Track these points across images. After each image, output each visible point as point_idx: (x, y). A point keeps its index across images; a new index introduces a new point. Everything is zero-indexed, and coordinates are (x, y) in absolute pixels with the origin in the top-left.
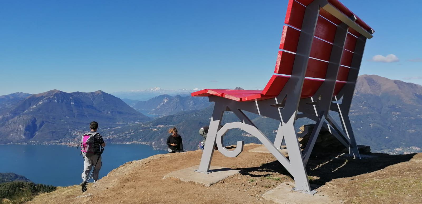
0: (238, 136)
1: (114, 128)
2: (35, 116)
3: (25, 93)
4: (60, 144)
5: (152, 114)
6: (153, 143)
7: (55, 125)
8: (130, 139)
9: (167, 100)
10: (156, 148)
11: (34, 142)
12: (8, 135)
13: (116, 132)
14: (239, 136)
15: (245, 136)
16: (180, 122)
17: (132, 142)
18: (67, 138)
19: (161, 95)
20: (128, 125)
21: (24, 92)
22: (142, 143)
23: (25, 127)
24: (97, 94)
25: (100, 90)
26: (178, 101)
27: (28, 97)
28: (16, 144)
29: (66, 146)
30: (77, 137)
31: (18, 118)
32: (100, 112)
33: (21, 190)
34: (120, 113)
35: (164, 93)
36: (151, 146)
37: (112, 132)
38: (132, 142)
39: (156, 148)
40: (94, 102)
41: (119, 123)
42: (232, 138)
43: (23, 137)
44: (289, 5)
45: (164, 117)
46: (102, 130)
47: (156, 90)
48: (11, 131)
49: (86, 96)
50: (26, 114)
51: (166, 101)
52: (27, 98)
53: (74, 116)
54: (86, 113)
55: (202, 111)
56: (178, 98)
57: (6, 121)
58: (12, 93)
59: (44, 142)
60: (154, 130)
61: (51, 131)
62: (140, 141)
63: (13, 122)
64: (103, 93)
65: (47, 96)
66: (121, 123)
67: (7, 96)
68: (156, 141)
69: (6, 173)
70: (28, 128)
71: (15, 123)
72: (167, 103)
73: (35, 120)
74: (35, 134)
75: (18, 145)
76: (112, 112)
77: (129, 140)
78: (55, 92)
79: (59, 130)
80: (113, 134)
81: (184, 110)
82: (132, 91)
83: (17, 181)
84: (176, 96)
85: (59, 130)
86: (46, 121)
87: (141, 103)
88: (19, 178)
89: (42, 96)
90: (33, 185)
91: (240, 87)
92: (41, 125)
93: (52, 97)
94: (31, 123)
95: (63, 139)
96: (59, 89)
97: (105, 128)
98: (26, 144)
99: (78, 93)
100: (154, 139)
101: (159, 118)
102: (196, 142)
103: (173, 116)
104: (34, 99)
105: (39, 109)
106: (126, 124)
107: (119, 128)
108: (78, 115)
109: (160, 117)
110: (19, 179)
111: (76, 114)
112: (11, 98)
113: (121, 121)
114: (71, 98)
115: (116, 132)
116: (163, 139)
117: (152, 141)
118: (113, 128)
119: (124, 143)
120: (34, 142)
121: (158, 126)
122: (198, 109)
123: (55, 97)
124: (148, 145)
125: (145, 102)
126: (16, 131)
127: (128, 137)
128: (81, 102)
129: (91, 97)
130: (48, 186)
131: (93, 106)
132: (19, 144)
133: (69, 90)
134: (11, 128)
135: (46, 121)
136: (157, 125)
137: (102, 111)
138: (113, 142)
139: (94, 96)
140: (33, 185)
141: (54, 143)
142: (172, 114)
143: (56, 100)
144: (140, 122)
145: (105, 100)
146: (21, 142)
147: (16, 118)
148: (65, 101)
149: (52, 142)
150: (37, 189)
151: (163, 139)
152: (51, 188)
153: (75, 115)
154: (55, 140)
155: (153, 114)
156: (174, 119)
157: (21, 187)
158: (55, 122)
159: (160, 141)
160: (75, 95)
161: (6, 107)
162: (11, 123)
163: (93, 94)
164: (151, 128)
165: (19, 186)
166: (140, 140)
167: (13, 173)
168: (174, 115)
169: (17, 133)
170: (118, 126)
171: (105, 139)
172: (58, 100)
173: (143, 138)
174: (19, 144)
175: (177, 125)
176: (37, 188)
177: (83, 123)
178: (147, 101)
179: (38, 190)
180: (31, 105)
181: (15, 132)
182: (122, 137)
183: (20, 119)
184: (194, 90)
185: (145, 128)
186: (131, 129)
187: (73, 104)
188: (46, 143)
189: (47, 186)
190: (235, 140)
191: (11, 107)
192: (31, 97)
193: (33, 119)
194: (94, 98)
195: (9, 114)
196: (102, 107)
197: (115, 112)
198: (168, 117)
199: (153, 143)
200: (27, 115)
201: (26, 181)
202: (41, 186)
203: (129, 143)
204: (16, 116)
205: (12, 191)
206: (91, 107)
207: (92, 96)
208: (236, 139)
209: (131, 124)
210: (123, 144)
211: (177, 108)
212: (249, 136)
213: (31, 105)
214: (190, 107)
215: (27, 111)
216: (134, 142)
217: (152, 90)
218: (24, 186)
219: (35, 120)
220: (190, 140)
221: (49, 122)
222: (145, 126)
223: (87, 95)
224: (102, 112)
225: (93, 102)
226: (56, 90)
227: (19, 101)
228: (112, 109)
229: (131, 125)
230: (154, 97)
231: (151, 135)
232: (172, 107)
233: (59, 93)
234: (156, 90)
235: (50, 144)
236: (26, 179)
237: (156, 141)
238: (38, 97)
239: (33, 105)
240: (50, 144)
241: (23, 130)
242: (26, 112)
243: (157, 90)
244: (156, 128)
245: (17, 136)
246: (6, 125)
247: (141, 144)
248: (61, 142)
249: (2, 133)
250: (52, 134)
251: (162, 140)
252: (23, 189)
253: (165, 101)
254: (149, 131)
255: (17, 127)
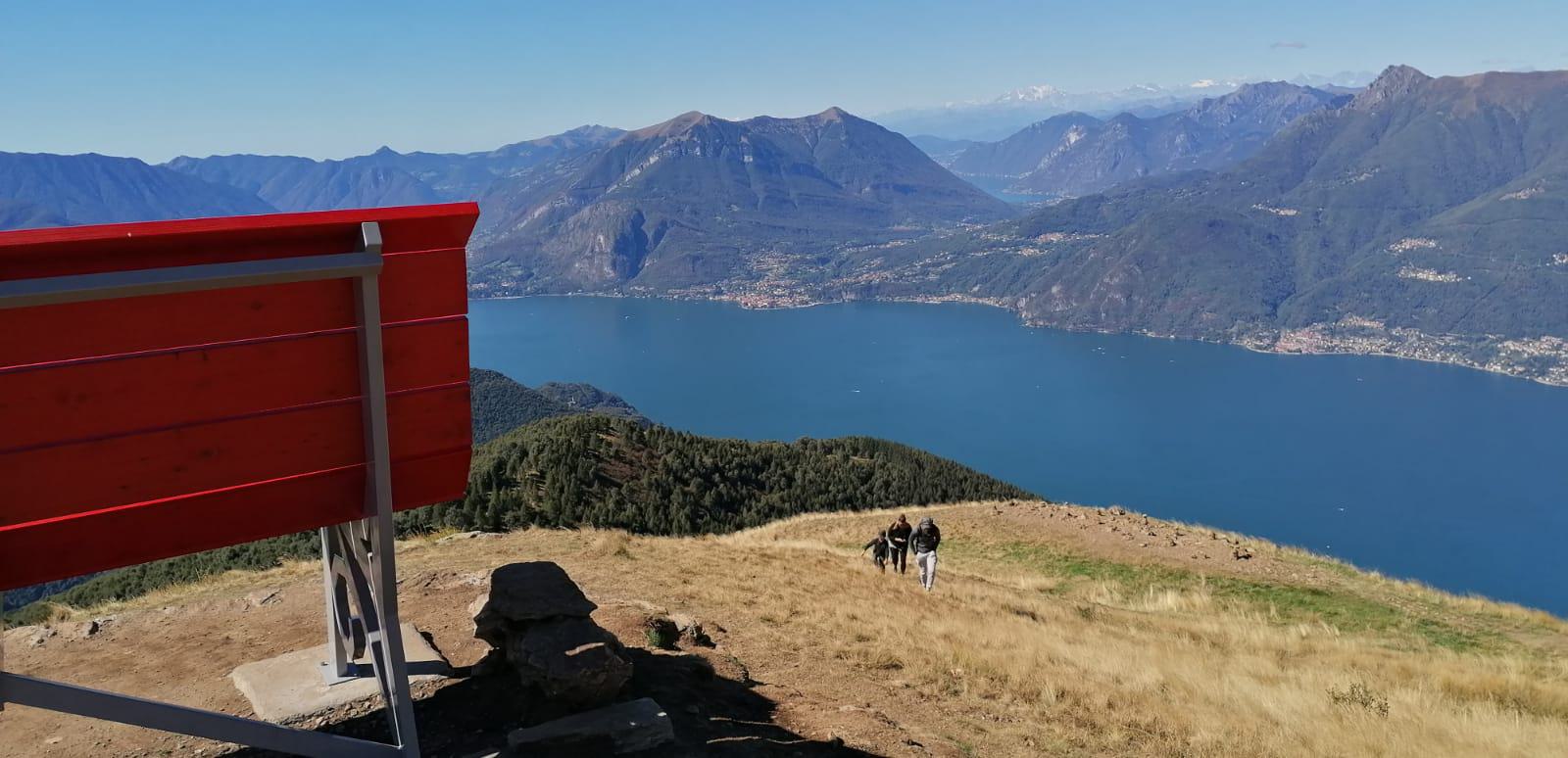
0: (1381, 278)
1: (882, 246)
2: (639, 206)
3: (606, 128)
4: (717, 298)
5: (1016, 191)
6: (1022, 303)
7: (699, 234)
8: (939, 285)
9: (1078, 134)
10: (1032, 320)
11: (642, 288)
12: (568, 266)
13: (892, 259)
14: (1385, 278)
15: (1415, 280)
16: (1128, 221)
17: (946, 298)
18: (738, 279)
19: (1056, 114)
20: (930, 236)
21: (603, 124)
22: (980, 301)
23: (612, 241)
24: (825, 122)
25: (835, 108)
26: (1124, 135)
27: (615, 143)
28: (592, 294)
29: (734, 304)
30: (766, 278)
31: (591, 210)
32: (837, 186)
33: (602, 440)
34: (904, 190)
35: (1067, 107)
36: (1014, 314)
37: (878, 261)
38: (946, 298)
39: (1032, 320)
40: (815, 152)
41: (902, 227)
42: (1354, 284)
43: (609, 274)
44: (15, 620)
45: (1063, 203)
46: (845, 254)
47: (1036, 95)
48: (574, 255)
49: (790, 129)
50: (614, 196)
51: (1073, 138)
52: (615, 145)
53: (756, 205)
54: (793, 194)
55: (1224, 177)
56: (1123, 124)
57: (559, 221)
58: (571, 129)
59: (669, 291)
60: (1027, 252)
61: (689, 255)
62: (974, 295)
63: (579, 224)
64: (845, 116)
65: (671, 137)
66: (909, 228)
67: (557, 140)
68: (1033, 295)
69: (571, 384)
70: (621, 246)
71: (584, 226)
72: (1081, 146)
73: (638, 220)
74: (642, 263)
75: (596, 296)
76: (875, 187)
77: (945, 283)
78: (695, 122)
79: (710, 253)
80: (880, 268)
81: (1146, 171)
82: (948, 105)
83: (599, 411)
84: (1117, 117)
85: (710, 253)
86: (673, 223)
87: (980, 152)
88: (605, 403)
89: (657, 137)
90: (638, 429)
91: (1406, 64)
92: (659, 236)
93: (684, 138)
94: (628, 227)
95: (726, 281)
96: (708, 109)
97: (854, 246)
98: (620, 296)
99: (762, 121)
100: (1025, 287)
101: (1046, 208)
102: (1190, 299)
103: (1102, 198)
104: (633, 146)
105: (649, 181)
106: (925, 232)
107: (899, 247)
108: (766, 198)
109: (1051, 203)
110: (607, 405)
111: (761, 196)
112: (569, 144)
113: (908, 219)
114: (744, 140)
115: (892, 259)
116: (1060, 287)
117: (1020, 294)
118: (881, 244)
119: (919, 300)
120: (642, 288)
121: (1041, 240)
122: (1207, 169)
123: (695, 139)
124: (1005, 309)
125: (996, 144)
126: (588, 253)
127: (932, 277)
128: (773, 152)
129: (807, 133)
130: (680, 434)
131: (815, 165)
132: (600, 294)
133: (736, 110)
134: (576, 244)
135: (673, 223)
136: (1038, 235)
137: (844, 185)
138: (882, 294)
139: (816, 131)
140: (638, 429)
141: (699, 293)
142: (1096, 192)
143: (698, 149)
144: (977, 223)
145: (851, 145)
146: (606, 290)
147: (586, 211)
148: (726, 151)
149: (692, 290)
150: (649, 441)
151: (1060, 287)
152: (688, 441)
153: (758, 201)
154: (701, 283)
155: (1024, 192)
156: (1105, 209)
157: (602, 432)
158: (698, 223)
159: (1048, 293)
160: (754, 131)
161: (557, 175)
162: (573, 229)
163: (813, 123)
164: (1016, 245)
165: (598, 429)
166: (976, 289)
167: (588, 386)
168: (1106, 195)
169: (591, 258)
170: (896, 239)
171: (855, 283)
172: (703, 149)
173: (985, 280)
174: (600, 294)
175: (1115, 233)
176: (647, 437)
177: (783, 228)
178: (1003, 141)
179: (652, 444)
180: (624, 166)
181: (587, 257)
182: (910, 279)
183: (597, 213)
184: (1196, 89)
185: (993, 245)
186: (944, 250)
187: (751, 160)
188: (675, 294)
189: (676, 434)
190: (1366, 295)
191: (571, 174)
192: (624, 141)
193: (635, 213)
194: (817, 136)
195: (565, 199)
196: (842, 168)
197: (888, 188)
198: (1081, 200)
199: (1022, 303)
200: (616, 202)
201: (626, 412)
202: (659, 432)
203: (935, 300)
204: (585, 205)
205: (577, 442)
206: (809, 170)
207: (809, 130)
208: (1370, 292)
209: (944, 232)
210: (916, 303)
211: (1118, 167)
212: (1431, 278)
213: (626, 168)
214: (1172, 159)
215: (616, 186)
216: (952, 296)
217: (1021, 96)
218: (612, 428)
219: (638, 220)
220: (1168, 290)
221: (682, 226)
222: (993, 238)
223: (792, 127)
224: (841, 188)
225: (812, 152)
226: (695, 113)
227: (592, 155)
228: (876, 177)
229: (941, 233)
230: (1027, 124)
231: (1016, 271)
232: (1097, 162)
233: (707, 122)
234: (1038, 98)
235: (686, 299)
236: (625, 405)
237: (1033, 295)
238: (646, 140)
239: (632, 168)
240: (686, 299)
241: (609, 250)
242: (614, 191)
243: (1041, 97)
244: (1035, 246)
245: (594, 271)
246: (560, 232)
247: (977, 303)
248: (720, 292)
249: (551, 260)
250: (690, 266)
251: (1054, 290)
252: (609, 438)
253: (1073, 141)
254: (1009, 257)
255: (591, 240)
